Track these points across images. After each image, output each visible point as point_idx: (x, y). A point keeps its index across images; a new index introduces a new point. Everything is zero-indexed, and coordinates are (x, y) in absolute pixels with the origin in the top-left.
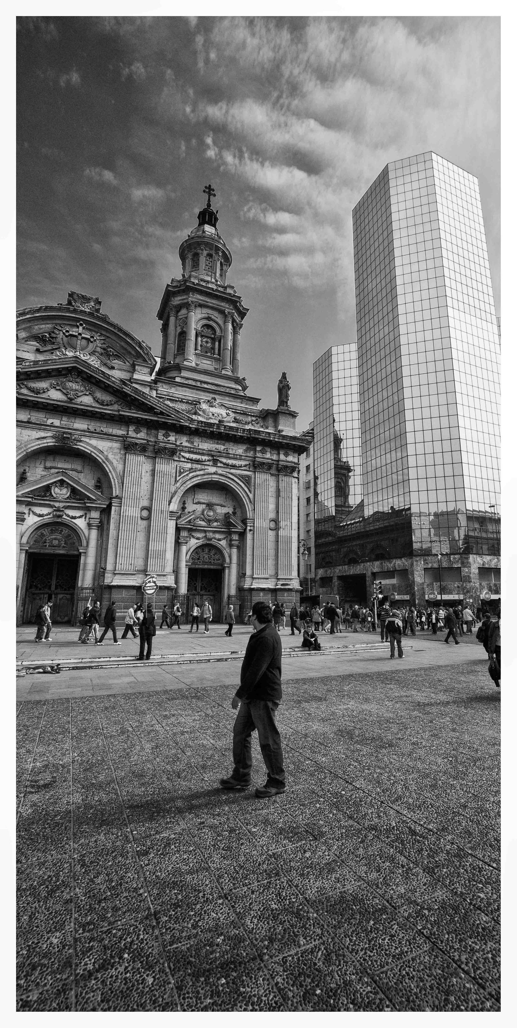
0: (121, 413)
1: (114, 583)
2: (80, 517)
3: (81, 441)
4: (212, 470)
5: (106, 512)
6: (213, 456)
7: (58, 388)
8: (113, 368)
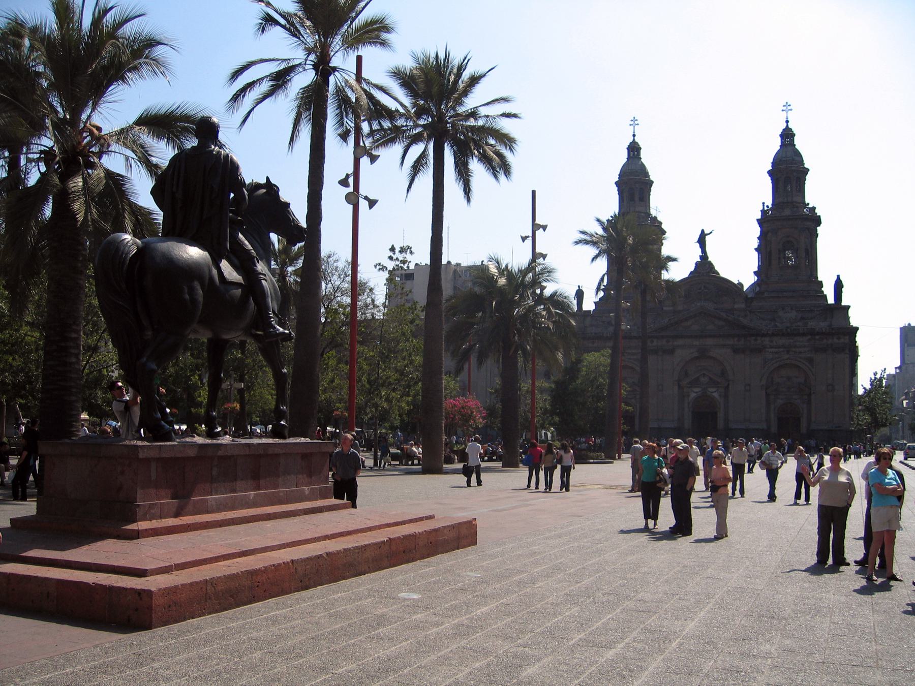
1: (733, 427)
2: (715, 392)
4: (787, 356)
5: (727, 388)
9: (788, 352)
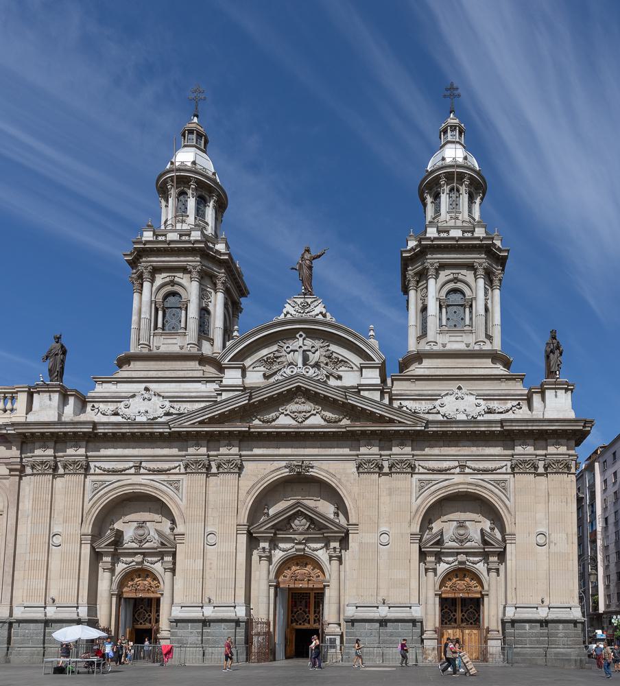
4: (457, 479)
5: (344, 542)
7: (285, 413)
8: (340, 378)
9: (463, 467)
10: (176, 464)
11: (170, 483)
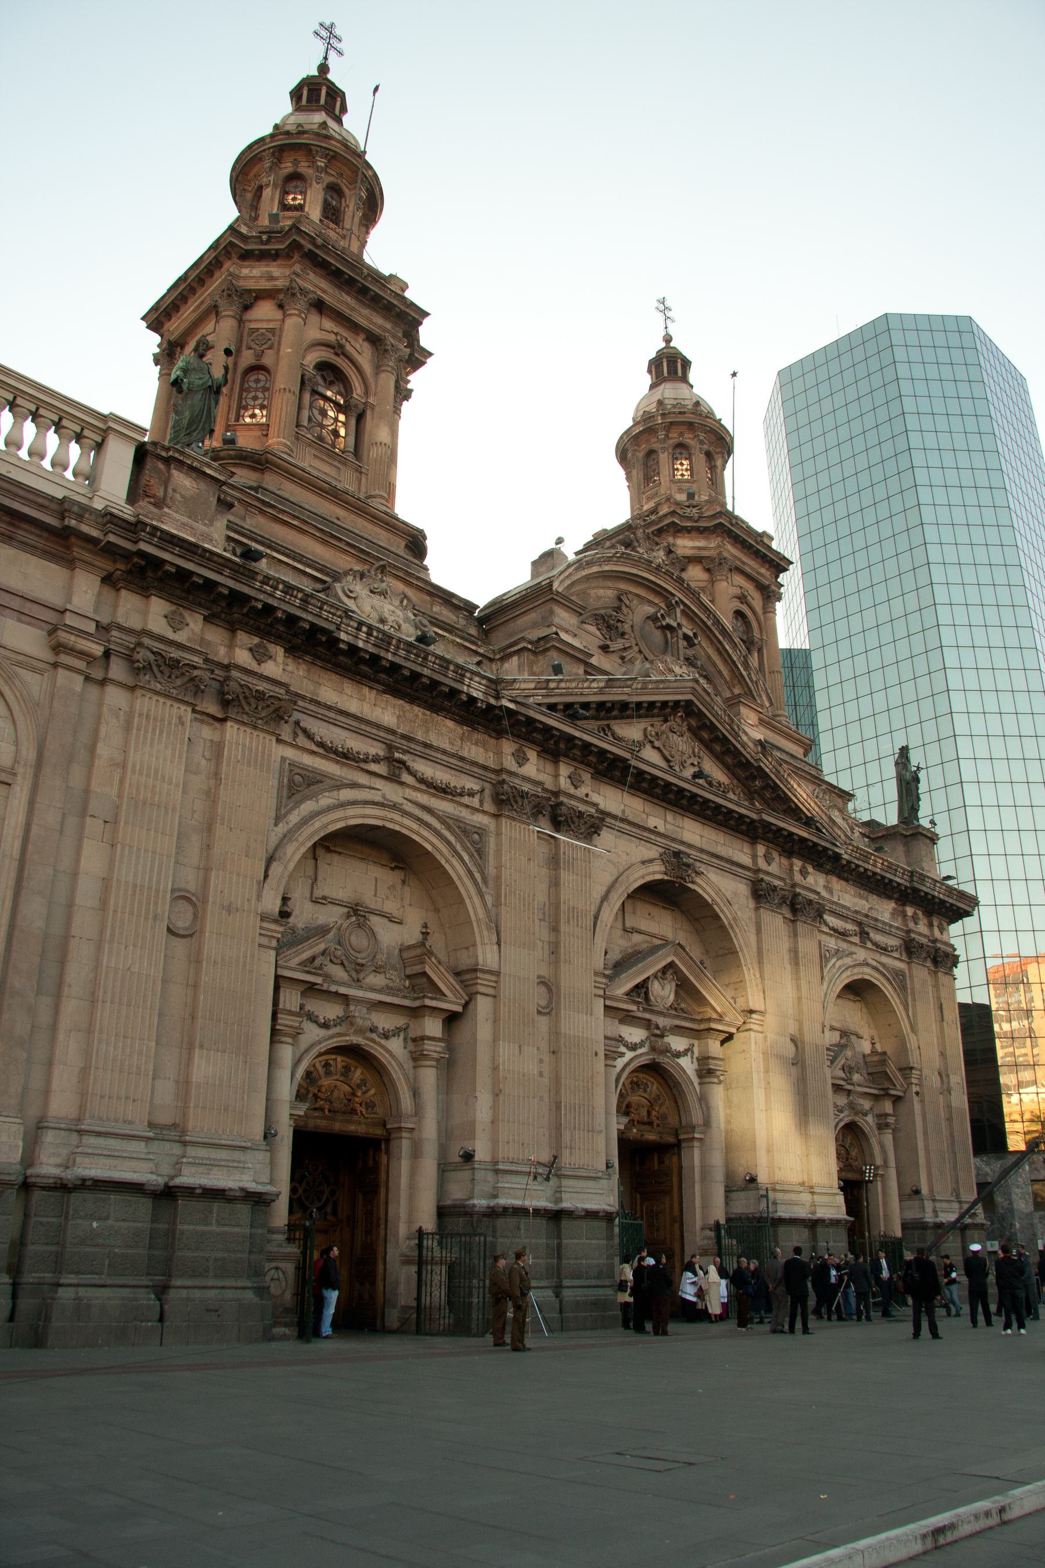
0: (765, 817)
3: (699, 873)
4: (861, 954)
6: (860, 924)
7: (657, 744)
10: (471, 784)
11: (464, 830)
